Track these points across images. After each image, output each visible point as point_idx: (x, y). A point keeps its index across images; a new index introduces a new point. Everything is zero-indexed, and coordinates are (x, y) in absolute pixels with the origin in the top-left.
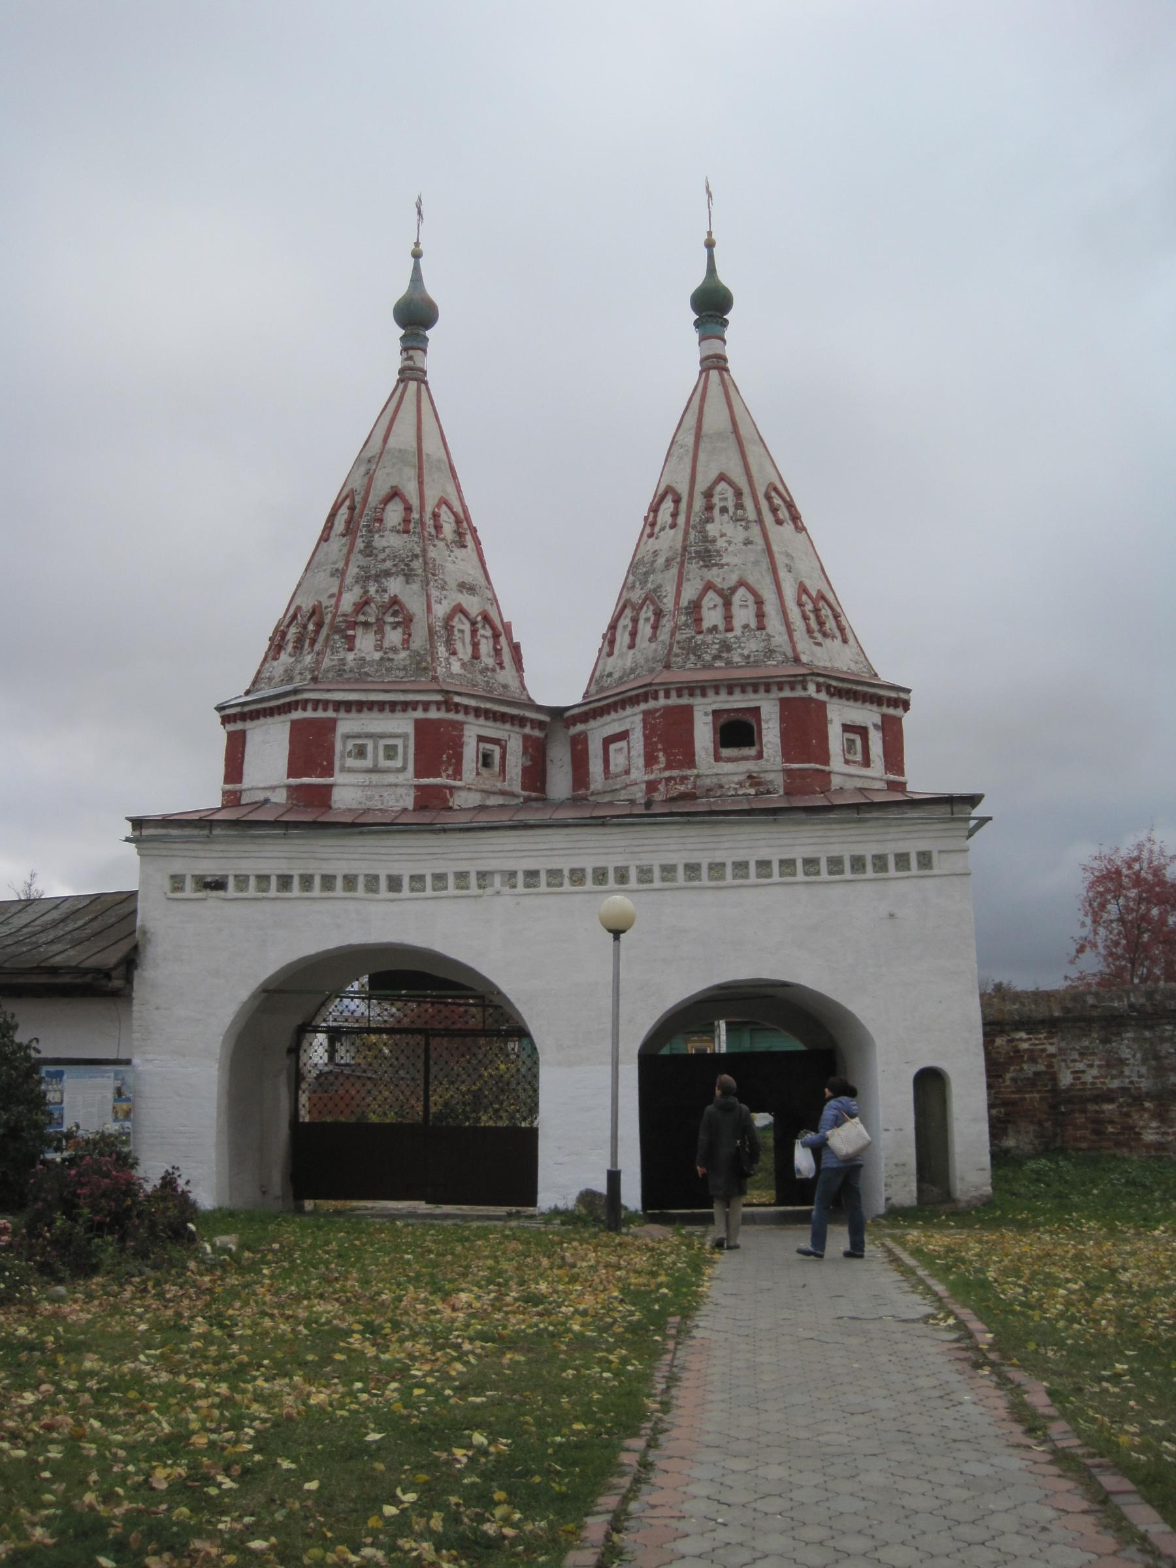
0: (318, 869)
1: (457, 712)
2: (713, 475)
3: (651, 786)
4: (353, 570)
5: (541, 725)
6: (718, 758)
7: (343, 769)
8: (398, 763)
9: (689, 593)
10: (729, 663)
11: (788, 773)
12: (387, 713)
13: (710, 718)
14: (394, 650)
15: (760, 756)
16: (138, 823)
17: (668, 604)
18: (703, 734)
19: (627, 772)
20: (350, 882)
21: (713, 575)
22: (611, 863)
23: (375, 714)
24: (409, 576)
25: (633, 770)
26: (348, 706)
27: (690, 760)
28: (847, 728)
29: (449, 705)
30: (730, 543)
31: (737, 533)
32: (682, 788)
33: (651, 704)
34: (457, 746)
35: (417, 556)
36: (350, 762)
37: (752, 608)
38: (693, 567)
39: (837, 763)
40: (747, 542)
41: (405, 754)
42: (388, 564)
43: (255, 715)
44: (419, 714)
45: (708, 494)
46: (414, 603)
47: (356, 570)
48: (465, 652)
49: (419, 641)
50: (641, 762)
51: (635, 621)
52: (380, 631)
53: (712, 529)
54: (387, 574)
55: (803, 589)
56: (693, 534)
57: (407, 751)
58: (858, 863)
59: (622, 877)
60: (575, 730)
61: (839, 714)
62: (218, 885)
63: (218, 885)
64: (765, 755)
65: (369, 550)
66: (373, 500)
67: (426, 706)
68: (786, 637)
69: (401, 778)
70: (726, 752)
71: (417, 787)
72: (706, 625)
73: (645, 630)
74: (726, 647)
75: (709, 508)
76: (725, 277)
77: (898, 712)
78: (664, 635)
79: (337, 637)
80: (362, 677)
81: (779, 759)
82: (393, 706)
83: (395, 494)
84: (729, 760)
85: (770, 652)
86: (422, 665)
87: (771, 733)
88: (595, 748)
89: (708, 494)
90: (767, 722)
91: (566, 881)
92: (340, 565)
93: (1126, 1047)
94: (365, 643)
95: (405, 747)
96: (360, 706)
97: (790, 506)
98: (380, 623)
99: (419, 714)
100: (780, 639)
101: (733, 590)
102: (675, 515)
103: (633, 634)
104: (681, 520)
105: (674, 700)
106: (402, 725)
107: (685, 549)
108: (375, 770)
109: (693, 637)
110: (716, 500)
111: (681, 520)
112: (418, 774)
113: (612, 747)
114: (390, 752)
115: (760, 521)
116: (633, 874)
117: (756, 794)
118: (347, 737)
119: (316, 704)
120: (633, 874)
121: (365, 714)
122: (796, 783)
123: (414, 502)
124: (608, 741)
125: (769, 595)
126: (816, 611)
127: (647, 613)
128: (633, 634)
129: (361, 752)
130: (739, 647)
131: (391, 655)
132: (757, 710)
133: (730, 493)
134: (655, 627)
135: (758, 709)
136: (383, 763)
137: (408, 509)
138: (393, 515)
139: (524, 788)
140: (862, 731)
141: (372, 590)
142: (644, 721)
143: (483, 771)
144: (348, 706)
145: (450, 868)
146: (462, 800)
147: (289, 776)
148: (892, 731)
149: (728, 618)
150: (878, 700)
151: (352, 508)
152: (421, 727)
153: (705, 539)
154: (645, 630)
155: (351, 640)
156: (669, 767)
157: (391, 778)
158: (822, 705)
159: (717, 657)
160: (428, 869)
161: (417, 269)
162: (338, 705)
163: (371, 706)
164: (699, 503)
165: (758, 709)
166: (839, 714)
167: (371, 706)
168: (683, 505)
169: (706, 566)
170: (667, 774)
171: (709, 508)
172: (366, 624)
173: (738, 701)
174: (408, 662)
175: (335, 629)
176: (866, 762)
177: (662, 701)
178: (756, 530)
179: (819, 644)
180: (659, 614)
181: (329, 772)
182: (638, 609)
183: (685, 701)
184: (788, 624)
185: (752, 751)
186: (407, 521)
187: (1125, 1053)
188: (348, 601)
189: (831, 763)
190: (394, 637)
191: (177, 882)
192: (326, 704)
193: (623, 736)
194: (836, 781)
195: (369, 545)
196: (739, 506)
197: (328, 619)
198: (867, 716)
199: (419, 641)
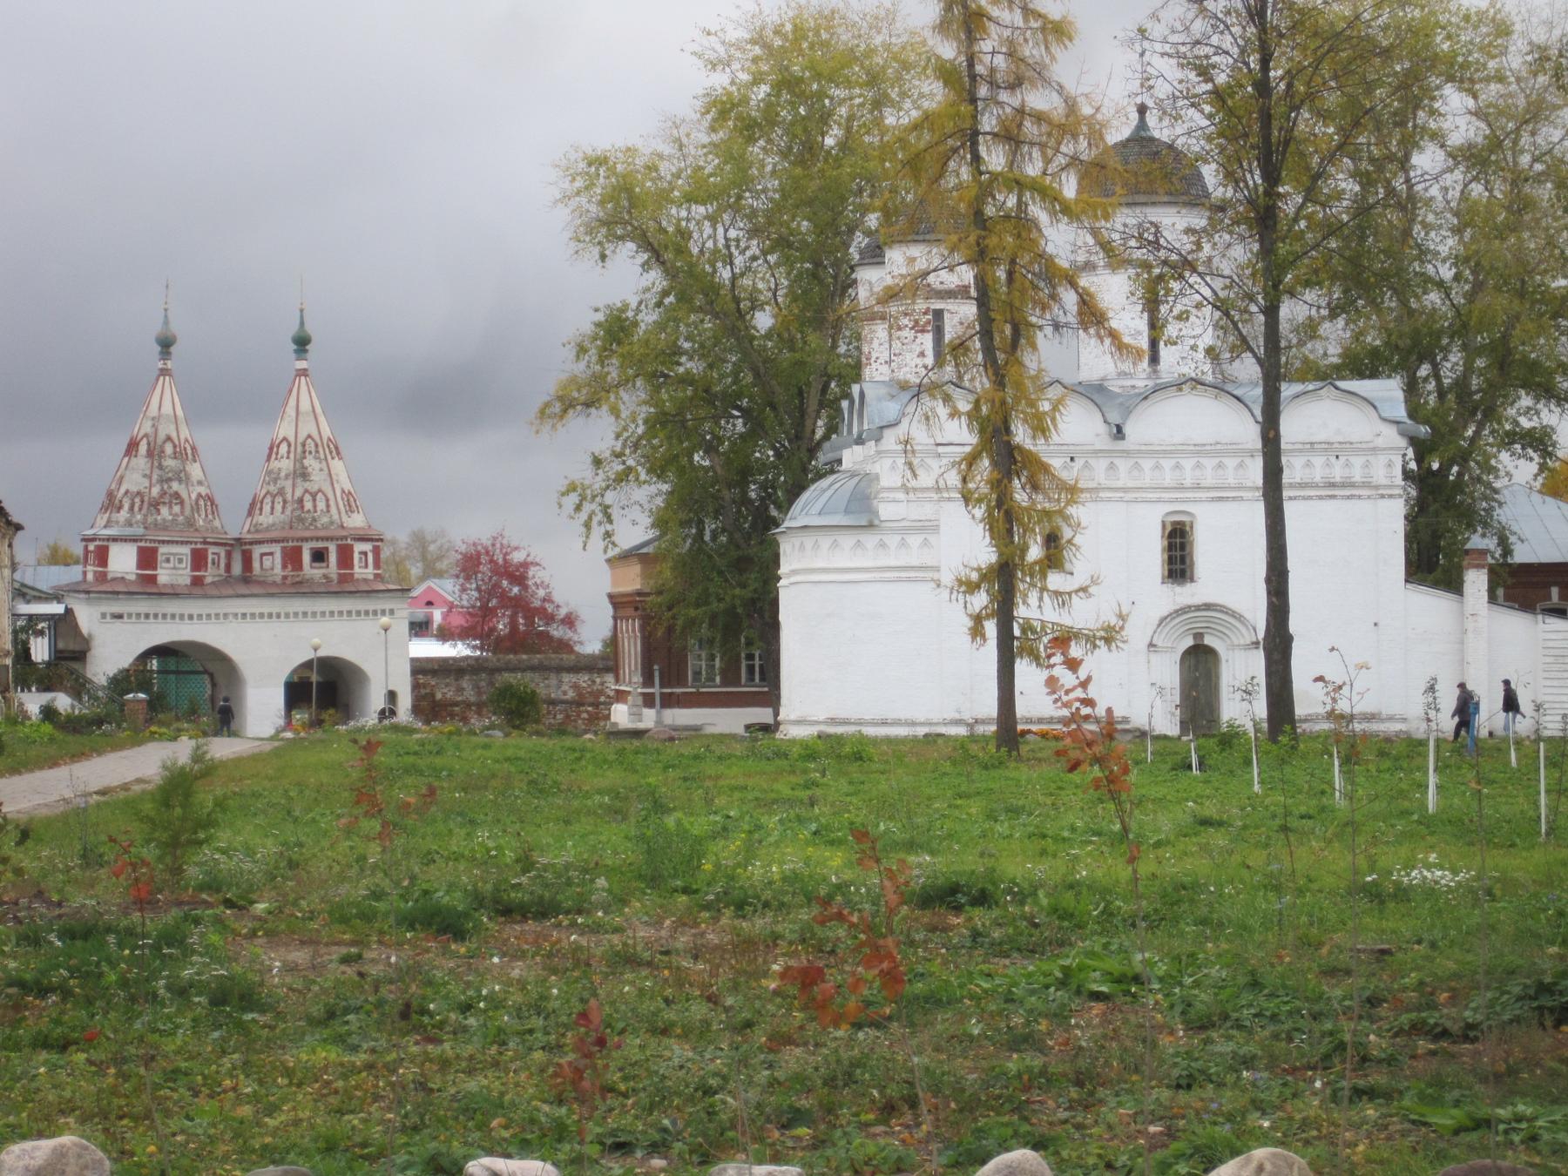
0: (161, 611)
3: (285, 578)
4: (155, 477)
9: (298, 493)
17: (289, 497)
18: (306, 557)
20: (173, 616)
21: (307, 485)
24: (180, 481)
26: (163, 542)
29: (205, 543)
34: (206, 558)
38: (299, 481)
39: (357, 569)
43: (115, 539)
46: (184, 495)
49: (188, 512)
53: (306, 462)
54: (170, 480)
58: (367, 613)
59: (278, 616)
61: (359, 547)
62: (120, 616)
63: (120, 616)
65: (161, 467)
73: (278, 507)
74: (314, 520)
78: (288, 512)
80: (165, 529)
83: (169, 438)
85: (332, 523)
86: (190, 523)
87: (333, 557)
89: (304, 445)
93: (466, 683)
94: (164, 511)
96: (168, 542)
100: (336, 517)
106: (185, 550)
114: (180, 561)
122: (343, 579)
124: (263, 555)
125: (331, 496)
127: (279, 499)
129: (168, 560)
138: (169, 449)
140: (365, 554)
144: (163, 542)
145: (213, 612)
146: (209, 580)
153: (304, 468)
154: (278, 507)
155: (158, 511)
160: (204, 612)
164: (299, 449)
166: (359, 547)
173: (320, 545)
175: (150, 505)
180: (285, 502)
181: (155, 568)
182: (274, 497)
187: (465, 685)
188: (155, 491)
190: (177, 509)
191: (104, 616)
193: (271, 554)
198: (367, 547)
199: (188, 512)
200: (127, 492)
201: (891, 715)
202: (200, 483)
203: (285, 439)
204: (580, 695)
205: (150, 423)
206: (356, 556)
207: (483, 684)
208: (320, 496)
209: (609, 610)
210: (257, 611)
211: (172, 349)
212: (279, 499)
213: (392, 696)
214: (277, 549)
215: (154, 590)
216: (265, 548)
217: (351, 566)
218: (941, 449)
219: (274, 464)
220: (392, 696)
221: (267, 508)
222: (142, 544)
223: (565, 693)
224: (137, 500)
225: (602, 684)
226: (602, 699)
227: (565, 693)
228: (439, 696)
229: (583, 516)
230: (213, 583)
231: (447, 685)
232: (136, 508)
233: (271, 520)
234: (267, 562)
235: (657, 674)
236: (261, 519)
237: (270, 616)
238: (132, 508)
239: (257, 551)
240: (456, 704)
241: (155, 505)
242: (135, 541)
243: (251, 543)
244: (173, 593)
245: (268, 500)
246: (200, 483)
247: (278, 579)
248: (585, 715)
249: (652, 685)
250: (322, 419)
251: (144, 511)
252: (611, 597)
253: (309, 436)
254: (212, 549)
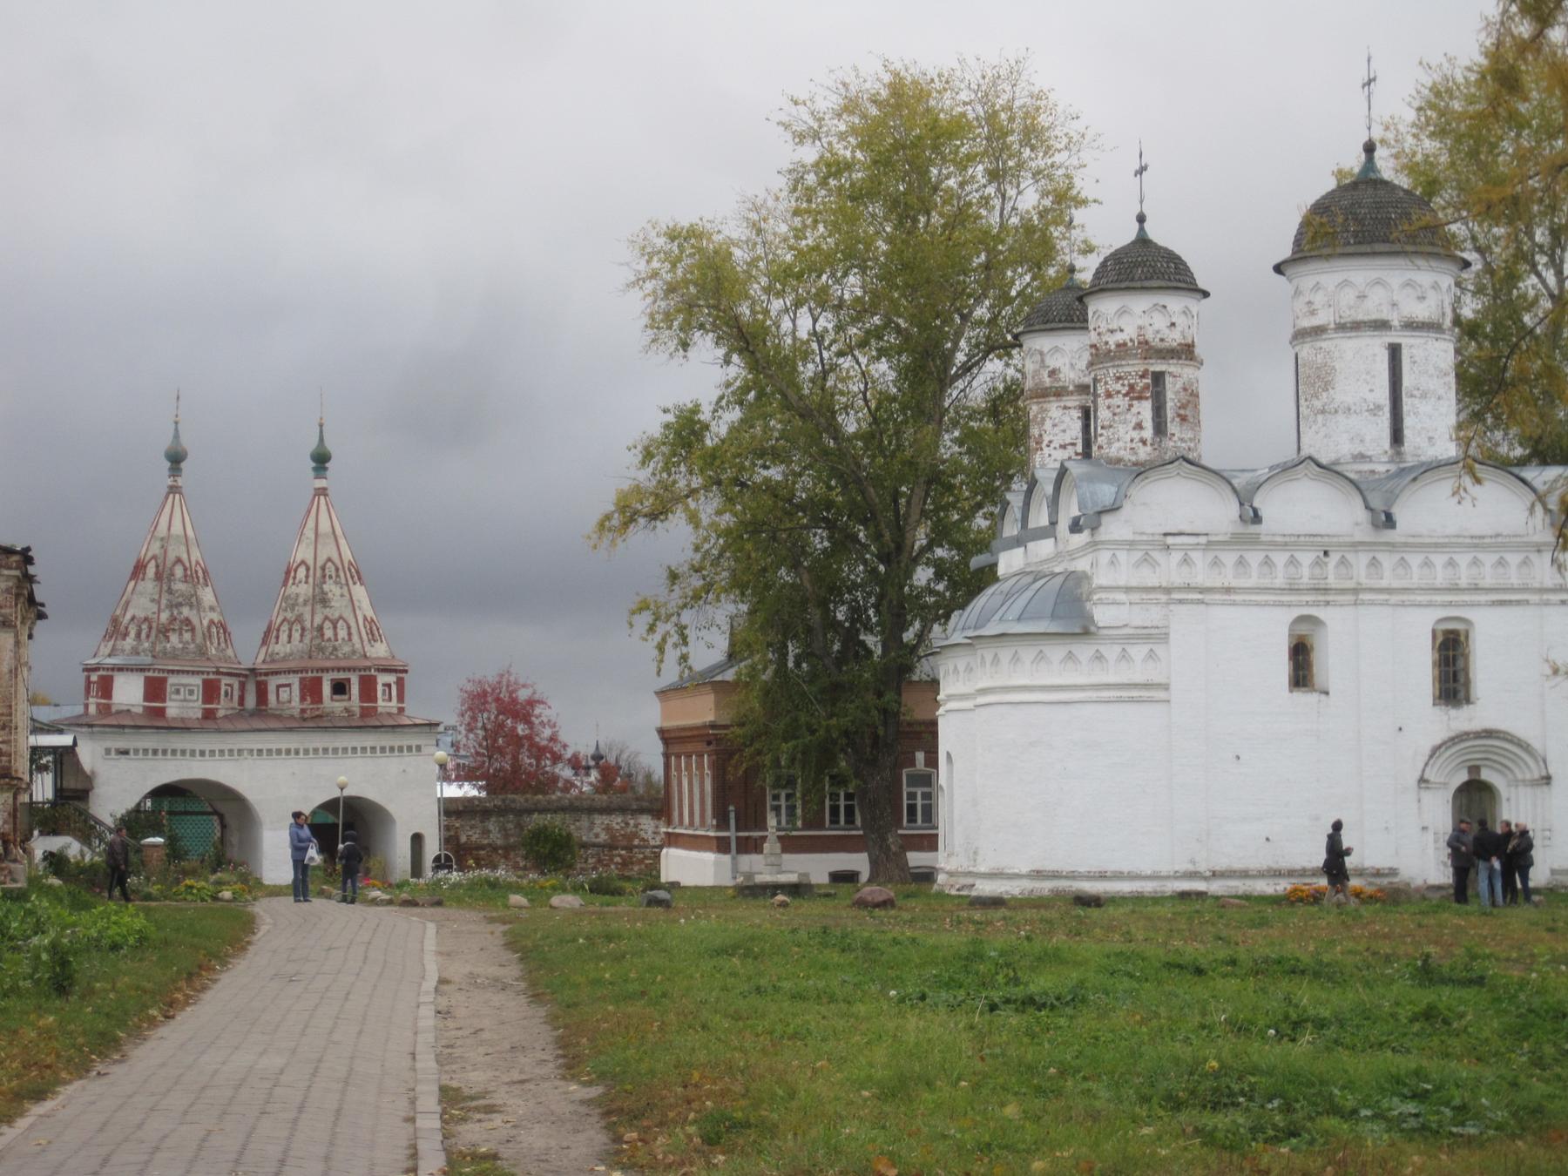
0: (170, 747)
2: (325, 557)
3: (303, 711)
4: (164, 602)
5: (246, 676)
6: (332, 700)
7: (171, 700)
9: (318, 620)
11: (362, 707)
14: (187, 643)
17: (308, 625)
18: (327, 689)
19: (290, 702)
20: (183, 752)
21: (327, 611)
22: (293, 746)
24: (191, 606)
26: (173, 672)
27: (320, 700)
28: (384, 685)
29: (218, 673)
31: (336, 590)
33: (304, 675)
36: (174, 697)
38: (318, 607)
39: (380, 703)
40: (342, 596)
42: (180, 599)
43: (120, 669)
45: (323, 568)
46: (195, 621)
48: (216, 644)
49: (199, 640)
50: (297, 699)
51: (290, 630)
52: (181, 634)
53: (326, 587)
54: (180, 605)
55: (365, 619)
56: (317, 590)
57: (199, 694)
58: (392, 749)
59: (297, 752)
60: (259, 679)
61: (383, 679)
62: (125, 752)
63: (125, 752)
65: (170, 591)
66: (169, 564)
67: (208, 673)
69: (196, 704)
70: (335, 697)
72: (326, 637)
73: (296, 635)
74: (335, 649)
75: (324, 576)
77: (404, 675)
78: (307, 640)
80: (175, 657)
83: (179, 560)
85: (354, 652)
86: (202, 652)
87: (355, 689)
88: (272, 688)
89: (323, 568)
92: (156, 597)
93: (492, 825)
94: (174, 638)
96: (178, 672)
97: (357, 572)
98: (181, 629)
99: (205, 676)
100: (358, 646)
102: (307, 577)
103: (290, 636)
104: (311, 580)
105: (315, 674)
106: (197, 681)
107: (314, 597)
108: (185, 700)
111: (311, 580)
112: (205, 702)
114: (191, 693)
115: (347, 584)
116: (301, 752)
119: (159, 670)
120: (301, 752)
121: (181, 675)
122: (365, 713)
123: (187, 565)
124: (279, 687)
125: (353, 624)
127: (297, 627)
128: (290, 636)
129: (178, 692)
133: (333, 569)
134: (302, 635)
136: (188, 697)
137: (185, 570)
138: (179, 571)
140: (389, 686)
141: (175, 612)
142: (301, 683)
144: (173, 672)
146: (221, 713)
148: (400, 683)
149: (336, 635)
150: (396, 671)
151: (157, 566)
152: (206, 683)
153: (323, 593)
154: (296, 635)
155: (167, 638)
157: (191, 704)
159: (331, 654)
160: (217, 747)
161: (176, 430)
163: (183, 672)
166: (383, 679)
167: (183, 672)
168: (311, 572)
171: (324, 576)
172: (174, 630)
173: (342, 675)
175: (159, 631)
176: (390, 699)
177: (310, 674)
178: (345, 588)
180: (303, 629)
181: (164, 701)
182: (291, 624)
183: (319, 674)
184: (361, 638)
185: (346, 697)
186: (186, 576)
187: (491, 827)
188: (164, 617)
190: (187, 636)
191: (108, 751)
192: (163, 671)
193: (289, 685)
194: (380, 710)
195: (169, 588)
196: (338, 576)
197: (154, 625)
198: (391, 678)
199: (199, 640)
200: (133, 618)
201: (1112, 867)
202: (212, 609)
203: (303, 562)
204: (613, 837)
205: (158, 544)
206: (380, 688)
207: (510, 826)
208: (341, 623)
209: (659, 747)
210: (274, 747)
211: (183, 465)
212: (297, 627)
213: (417, 839)
214: (295, 680)
216: (282, 680)
217: (375, 700)
218: (1170, 540)
219: (292, 589)
220: (417, 839)
221: (284, 637)
222: (150, 674)
223: (597, 836)
224: (145, 627)
225: (636, 826)
226: (636, 842)
227: (597, 836)
228: (463, 839)
229: (657, 637)
230: (226, 717)
231: (472, 827)
232: (143, 635)
233: (288, 648)
234: (284, 693)
235: (732, 815)
236: (278, 648)
237: (288, 752)
238: (138, 635)
239: (273, 683)
240: (482, 847)
241: (164, 632)
242: (142, 670)
243: (266, 674)
244: (183, 728)
245: (285, 627)
246: (212, 609)
247: (296, 713)
248: (618, 859)
249: (727, 828)
250: (342, 542)
251: (153, 637)
252: (662, 733)
253: (329, 560)
254: (225, 680)
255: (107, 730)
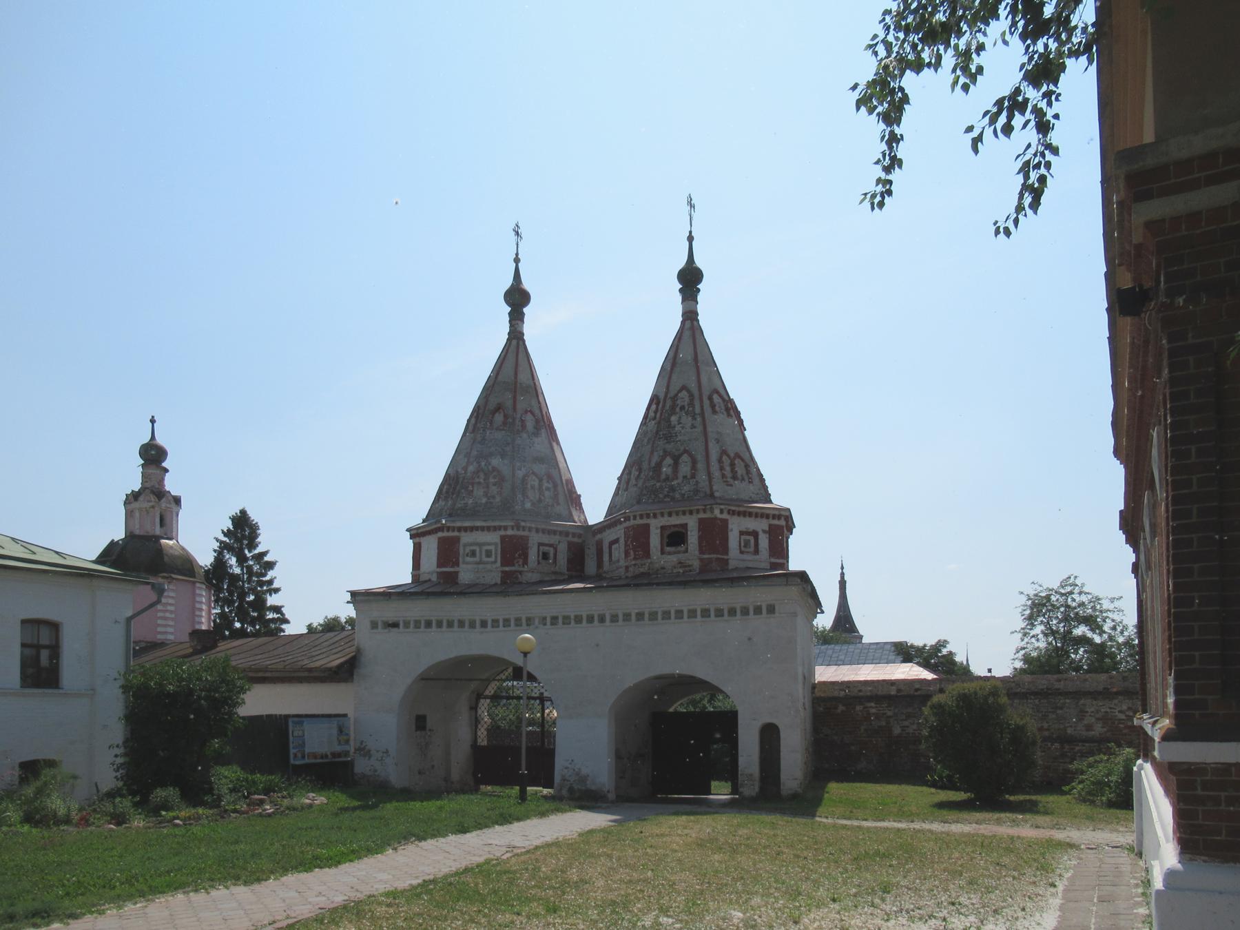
1: (524, 530)
6: (663, 552)
7: (464, 563)
8: (493, 559)
10: (673, 499)
11: (701, 560)
12: (486, 532)
13: (659, 531)
14: (494, 497)
15: (686, 551)
16: (354, 594)
18: (655, 540)
23: (479, 533)
25: (621, 560)
26: (466, 529)
27: (647, 554)
30: (683, 428)
31: (687, 420)
32: (642, 570)
35: (508, 444)
36: (468, 559)
37: (689, 464)
40: (693, 427)
41: (496, 554)
44: (502, 533)
47: (476, 453)
50: (623, 556)
64: (689, 550)
67: (506, 528)
68: (707, 483)
70: (668, 549)
71: (502, 572)
76: (699, 262)
79: (463, 491)
81: (697, 552)
82: (488, 529)
84: (669, 553)
85: (696, 491)
87: (693, 538)
89: (675, 398)
90: (691, 531)
91: (573, 622)
94: (479, 492)
95: (496, 550)
99: (502, 533)
101: (680, 456)
105: (639, 521)
108: (480, 562)
109: (655, 484)
110: (679, 402)
112: (503, 565)
113: (614, 547)
114: (488, 554)
115: (702, 414)
117: (684, 572)
118: (465, 545)
125: (700, 457)
126: (732, 465)
129: (473, 554)
130: (680, 489)
131: (491, 500)
132: (685, 526)
133: (687, 400)
135: (686, 524)
139: (568, 570)
140: (755, 534)
143: (543, 562)
144: (466, 529)
147: (437, 567)
156: (635, 559)
157: (489, 566)
158: (725, 522)
159: (667, 496)
162: (459, 529)
165: (686, 524)
166: (736, 525)
169: (667, 443)
170: (633, 562)
174: (500, 504)
176: (756, 551)
179: (731, 485)
181: (457, 564)
183: (645, 521)
184: (709, 474)
185: (682, 548)
189: (730, 554)
192: (453, 529)
208: (685, 458)
215: (459, 590)
222: (445, 534)
255: (371, 598)
